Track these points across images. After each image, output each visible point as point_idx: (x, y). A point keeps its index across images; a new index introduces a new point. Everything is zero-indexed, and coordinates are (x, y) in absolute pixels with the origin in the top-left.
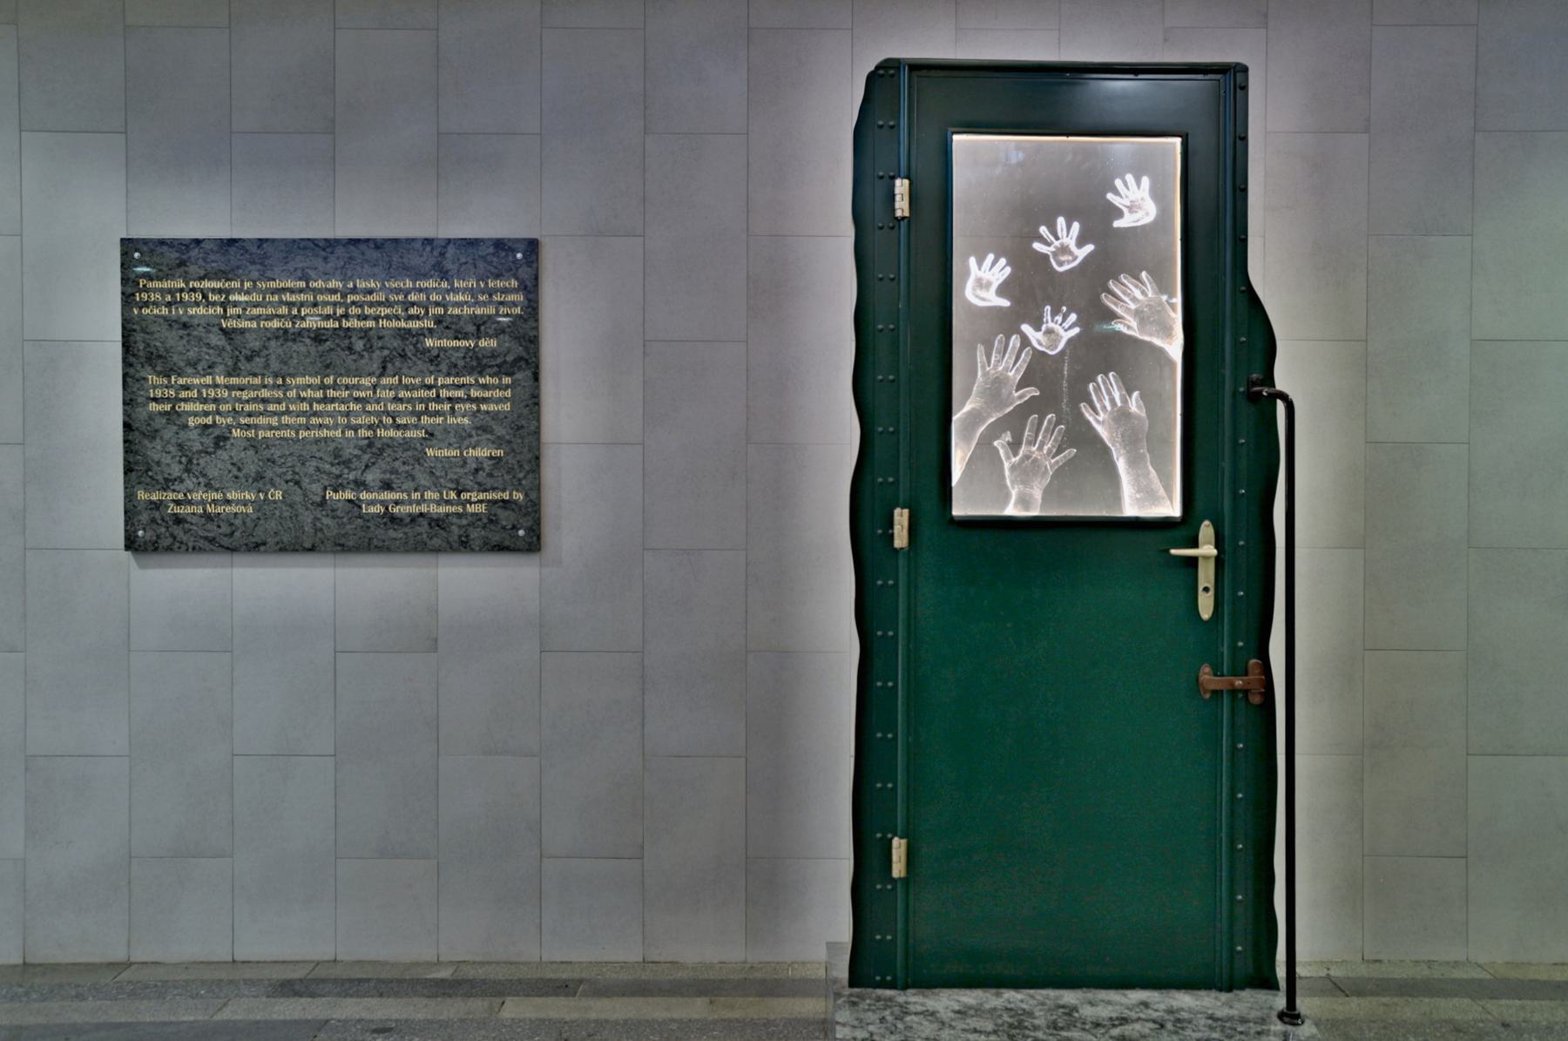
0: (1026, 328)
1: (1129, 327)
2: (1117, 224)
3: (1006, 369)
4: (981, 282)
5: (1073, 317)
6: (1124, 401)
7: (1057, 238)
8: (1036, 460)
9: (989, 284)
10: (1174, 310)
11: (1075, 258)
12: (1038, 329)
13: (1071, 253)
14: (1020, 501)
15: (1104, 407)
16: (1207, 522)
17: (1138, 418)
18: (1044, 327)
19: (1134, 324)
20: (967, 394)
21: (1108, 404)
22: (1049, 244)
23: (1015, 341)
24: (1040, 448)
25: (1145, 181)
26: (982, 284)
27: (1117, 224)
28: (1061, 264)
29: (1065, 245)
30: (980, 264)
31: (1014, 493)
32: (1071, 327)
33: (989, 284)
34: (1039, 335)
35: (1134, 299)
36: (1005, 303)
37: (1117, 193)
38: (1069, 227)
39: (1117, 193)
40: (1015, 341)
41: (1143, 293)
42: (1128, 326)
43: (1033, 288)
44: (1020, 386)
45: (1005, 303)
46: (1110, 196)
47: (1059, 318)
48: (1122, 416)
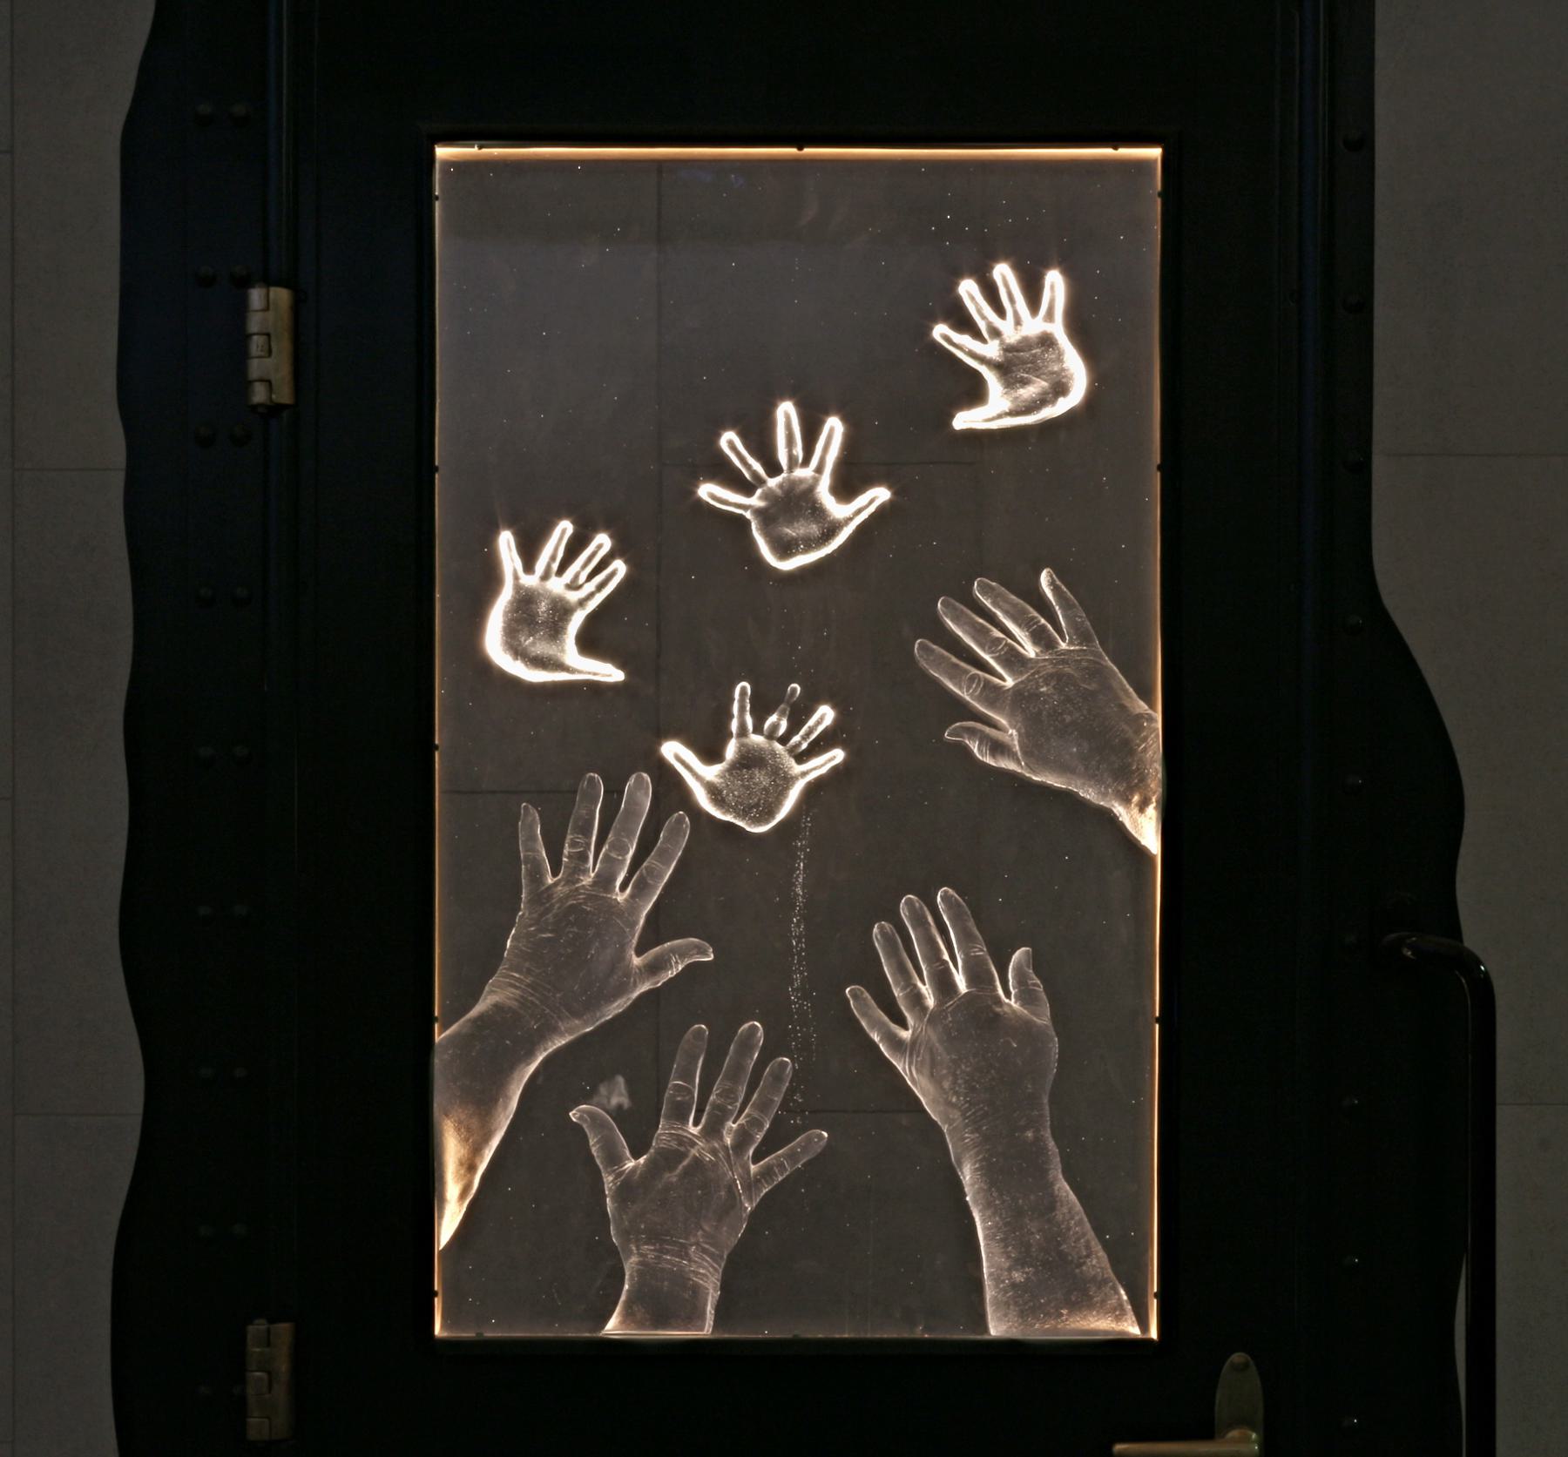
0: (671, 750)
1: (998, 748)
2: (964, 420)
3: (605, 881)
4: (540, 605)
5: (825, 715)
6: (977, 975)
7: (773, 468)
8: (698, 1162)
9: (562, 611)
10: (1145, 694)
11: (832, 530)
12: (711, 754)
13: (818, 512)
14: (671, 1292)
15: (916, 999)
16: (1237, 1357)
17: (1025, 1030)
18: (731, 750)
19: (1012, 735)
20: (481, 963)
21: (934, 982)
22: (746, 488)
23: (640, 791)
24: (713, 1131)
25: (1055, 283)
26: (535, 619)
27: (964, 420)
28: (785, 548)
29: (803, 486)
30: (528, 557)
31: (630, 1265)
32: (819, 746)
33: (562, 611)
34: (712, 772)
35: (1013, 660)
36: (610, 673)
37: (964, 323)
38: (811, 433)
39: (964, 323)
40: (640, 791)
41: (1039, 637)
42: (1003, 745)
43: (698, 622)
44: (656, 932)
45: (610, 673)
46: (940, 331)
47: (778, 721)
48: (974, 1020)
